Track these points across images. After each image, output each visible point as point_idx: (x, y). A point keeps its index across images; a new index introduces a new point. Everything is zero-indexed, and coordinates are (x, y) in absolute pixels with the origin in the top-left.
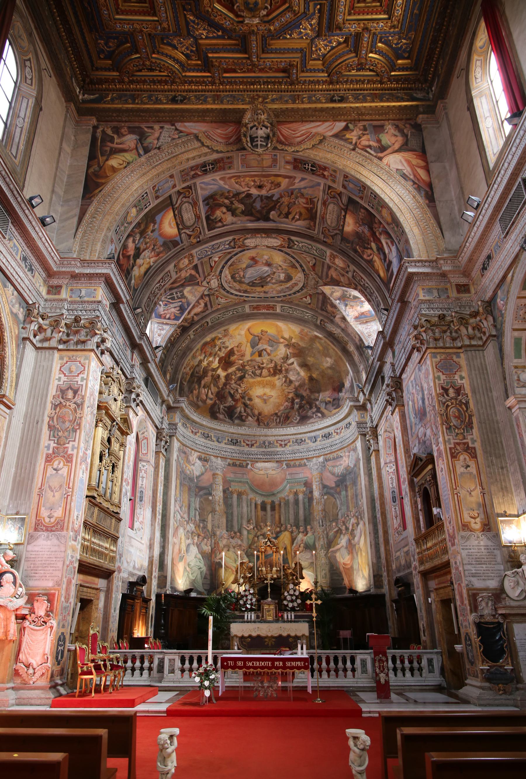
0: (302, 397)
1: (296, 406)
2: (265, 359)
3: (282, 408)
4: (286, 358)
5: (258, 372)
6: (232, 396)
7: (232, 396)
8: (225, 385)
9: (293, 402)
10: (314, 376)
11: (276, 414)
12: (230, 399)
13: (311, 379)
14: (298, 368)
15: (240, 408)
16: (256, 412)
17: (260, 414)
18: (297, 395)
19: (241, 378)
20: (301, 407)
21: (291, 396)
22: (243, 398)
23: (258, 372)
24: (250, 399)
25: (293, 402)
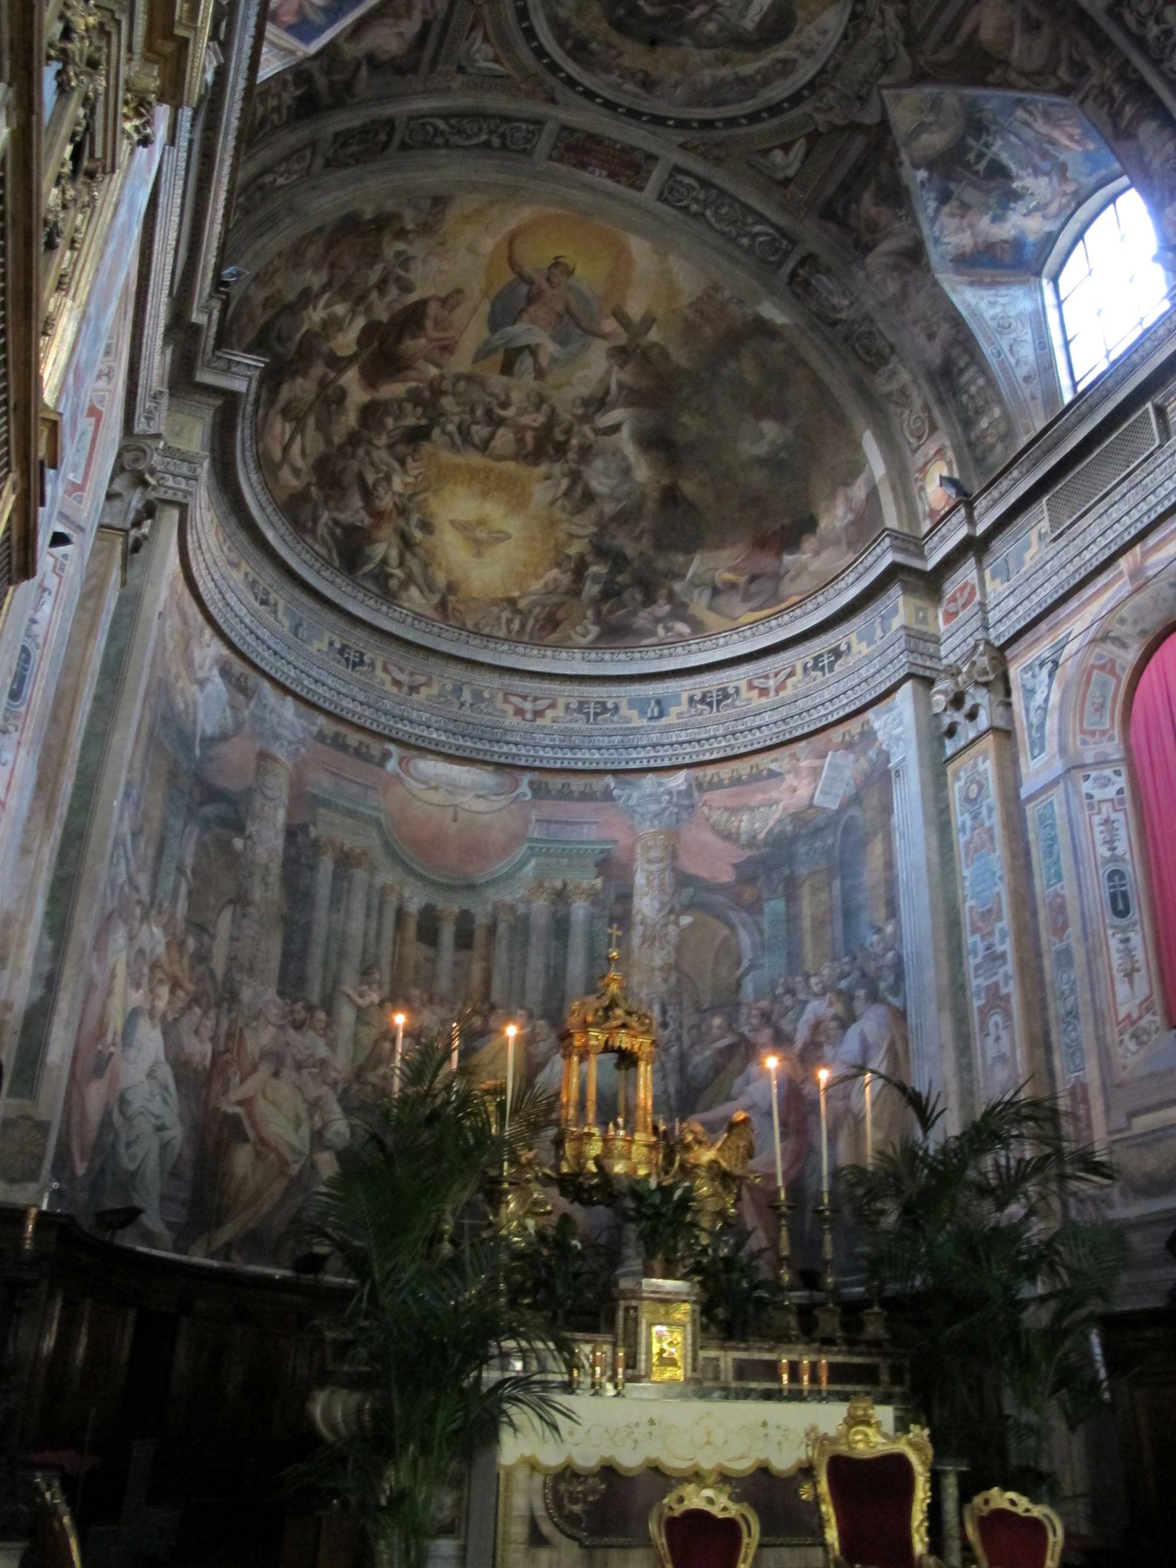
0: (618, 561)
1: (591, 589)
2: (521, 387)
3: (536, 586)
4: (599, 402)
5: (479, 432)
6: (368, 494)
7: (368, 494)
8: (353, 439)
9: (579, 570)
10: (688, 488)
11: (512, 602)
12: (357, 501)
13: (671, 497)
14: (630, 450)
15: (384, 548)
16: (441, 579)
17: (452, 588)
18: (601, 551)
19: (416, 436)
20: (610, 593)
21: (574, 549)
22: (403, 511)
23: (479, 432)
24: (426, 526)
25: (579, 570)
